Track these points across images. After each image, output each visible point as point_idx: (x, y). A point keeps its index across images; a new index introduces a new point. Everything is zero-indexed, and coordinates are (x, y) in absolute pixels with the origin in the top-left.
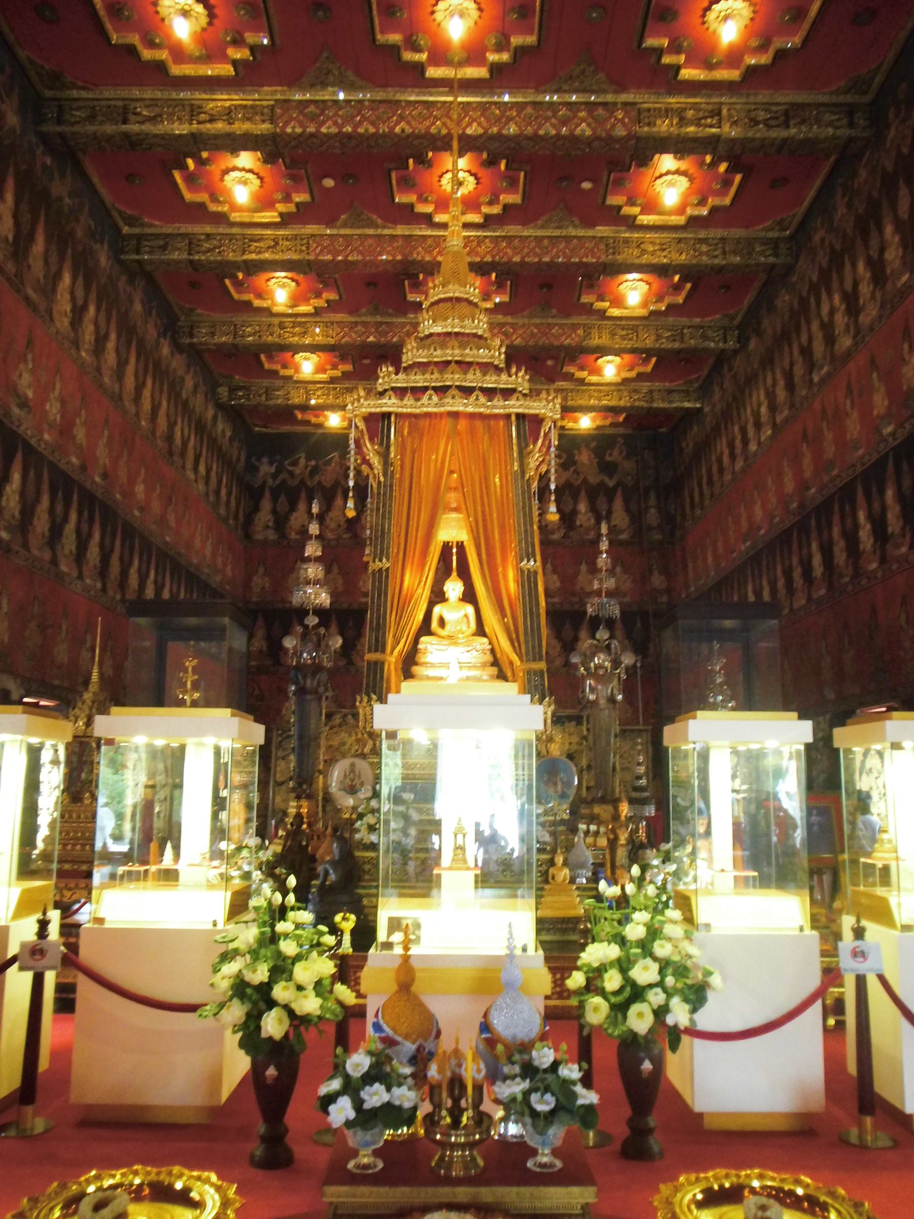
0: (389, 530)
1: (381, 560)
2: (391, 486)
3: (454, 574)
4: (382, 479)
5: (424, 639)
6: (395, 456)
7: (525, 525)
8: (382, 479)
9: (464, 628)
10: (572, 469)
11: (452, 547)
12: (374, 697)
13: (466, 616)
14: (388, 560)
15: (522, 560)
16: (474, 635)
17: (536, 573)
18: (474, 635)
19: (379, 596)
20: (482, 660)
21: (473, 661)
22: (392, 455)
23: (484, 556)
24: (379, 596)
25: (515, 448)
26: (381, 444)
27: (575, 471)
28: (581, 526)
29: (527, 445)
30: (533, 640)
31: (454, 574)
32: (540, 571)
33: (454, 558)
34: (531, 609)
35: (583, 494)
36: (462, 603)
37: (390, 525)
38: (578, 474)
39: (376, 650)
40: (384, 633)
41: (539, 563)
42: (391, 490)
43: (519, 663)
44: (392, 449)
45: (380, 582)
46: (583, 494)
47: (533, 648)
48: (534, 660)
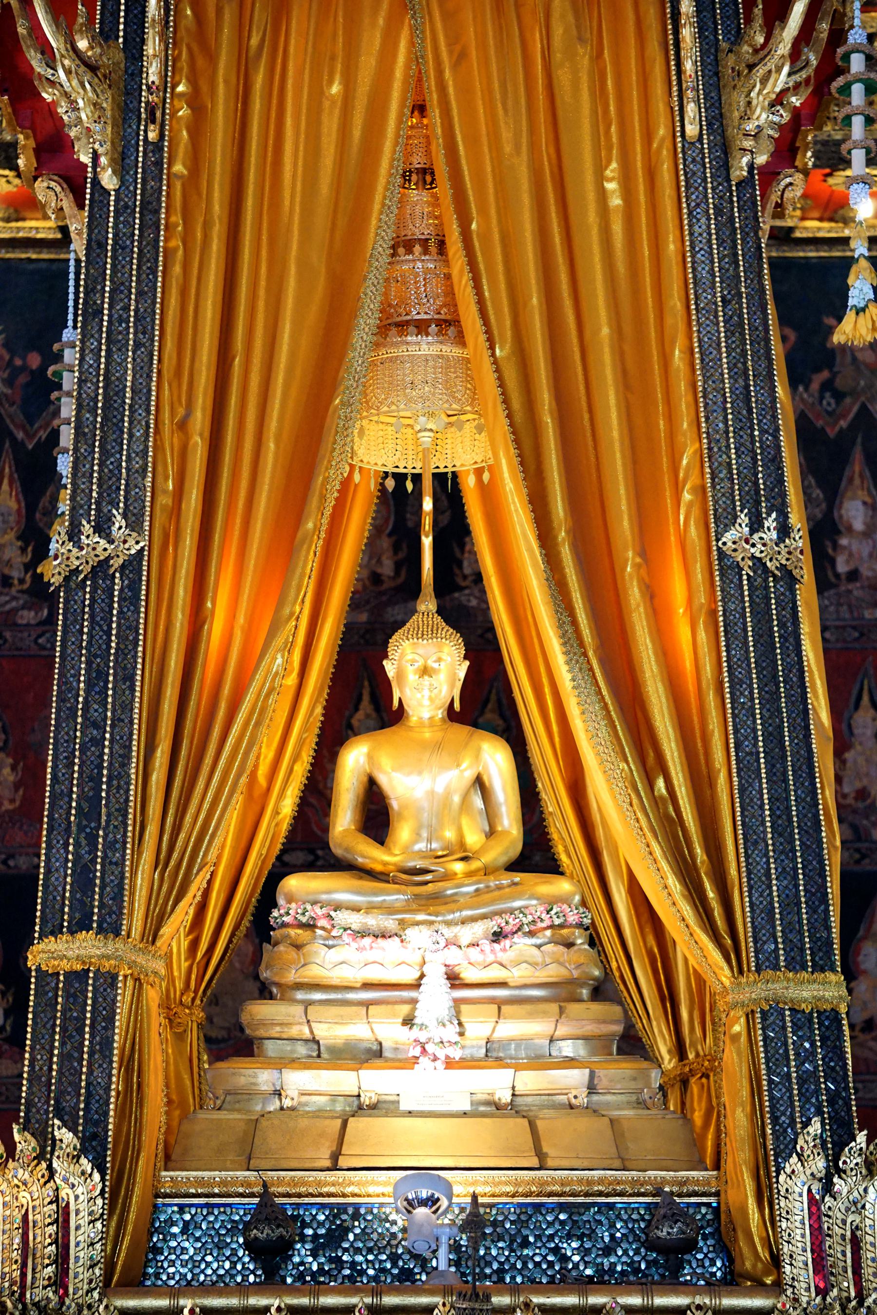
0: (141, 392)
1: (102, 528)
2: (150, 207)
3: (427, 604)
4: (109, 180)
5: (293, 883)
6: (166, 85)
7: (739, 372)
8: (109, 180)
9: (474, 838)
10: (819, 379)
11: (418, 495)
12: (66, 1136)
13: (480, 783)
14: (134, 524)
15: (726, 520)
16: (514, 866)
17: (789, 578)
18: (514, 866)
19: (97, 677)
20: (552, 973)
21: (518, 974)
22: (153, 73)
23: (559, 508)
24: (97, 677)
25: (687, 33)
26: (107, 35)
27: (827, 386)
28: (853, 575)
29: (737, 37)
30: (788, 874)
31: (427, 604)
32: (806, 574)
33: (427, 542)
34: (774, 737)
35: (857, 464)
36: (462, 731)
37: (143, 370)
38: (839, 396)
39: (81, 924)
40: (116, 845)
41: (799, 540)
42: (151, 225)
43: (725, 975)
44: (152, 46)
45: (100, 622)
46: (857, 464)
47: (790, 903)
48: (795, 964)
